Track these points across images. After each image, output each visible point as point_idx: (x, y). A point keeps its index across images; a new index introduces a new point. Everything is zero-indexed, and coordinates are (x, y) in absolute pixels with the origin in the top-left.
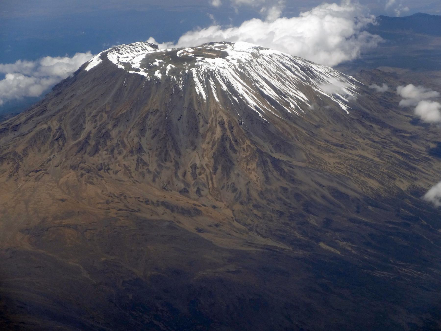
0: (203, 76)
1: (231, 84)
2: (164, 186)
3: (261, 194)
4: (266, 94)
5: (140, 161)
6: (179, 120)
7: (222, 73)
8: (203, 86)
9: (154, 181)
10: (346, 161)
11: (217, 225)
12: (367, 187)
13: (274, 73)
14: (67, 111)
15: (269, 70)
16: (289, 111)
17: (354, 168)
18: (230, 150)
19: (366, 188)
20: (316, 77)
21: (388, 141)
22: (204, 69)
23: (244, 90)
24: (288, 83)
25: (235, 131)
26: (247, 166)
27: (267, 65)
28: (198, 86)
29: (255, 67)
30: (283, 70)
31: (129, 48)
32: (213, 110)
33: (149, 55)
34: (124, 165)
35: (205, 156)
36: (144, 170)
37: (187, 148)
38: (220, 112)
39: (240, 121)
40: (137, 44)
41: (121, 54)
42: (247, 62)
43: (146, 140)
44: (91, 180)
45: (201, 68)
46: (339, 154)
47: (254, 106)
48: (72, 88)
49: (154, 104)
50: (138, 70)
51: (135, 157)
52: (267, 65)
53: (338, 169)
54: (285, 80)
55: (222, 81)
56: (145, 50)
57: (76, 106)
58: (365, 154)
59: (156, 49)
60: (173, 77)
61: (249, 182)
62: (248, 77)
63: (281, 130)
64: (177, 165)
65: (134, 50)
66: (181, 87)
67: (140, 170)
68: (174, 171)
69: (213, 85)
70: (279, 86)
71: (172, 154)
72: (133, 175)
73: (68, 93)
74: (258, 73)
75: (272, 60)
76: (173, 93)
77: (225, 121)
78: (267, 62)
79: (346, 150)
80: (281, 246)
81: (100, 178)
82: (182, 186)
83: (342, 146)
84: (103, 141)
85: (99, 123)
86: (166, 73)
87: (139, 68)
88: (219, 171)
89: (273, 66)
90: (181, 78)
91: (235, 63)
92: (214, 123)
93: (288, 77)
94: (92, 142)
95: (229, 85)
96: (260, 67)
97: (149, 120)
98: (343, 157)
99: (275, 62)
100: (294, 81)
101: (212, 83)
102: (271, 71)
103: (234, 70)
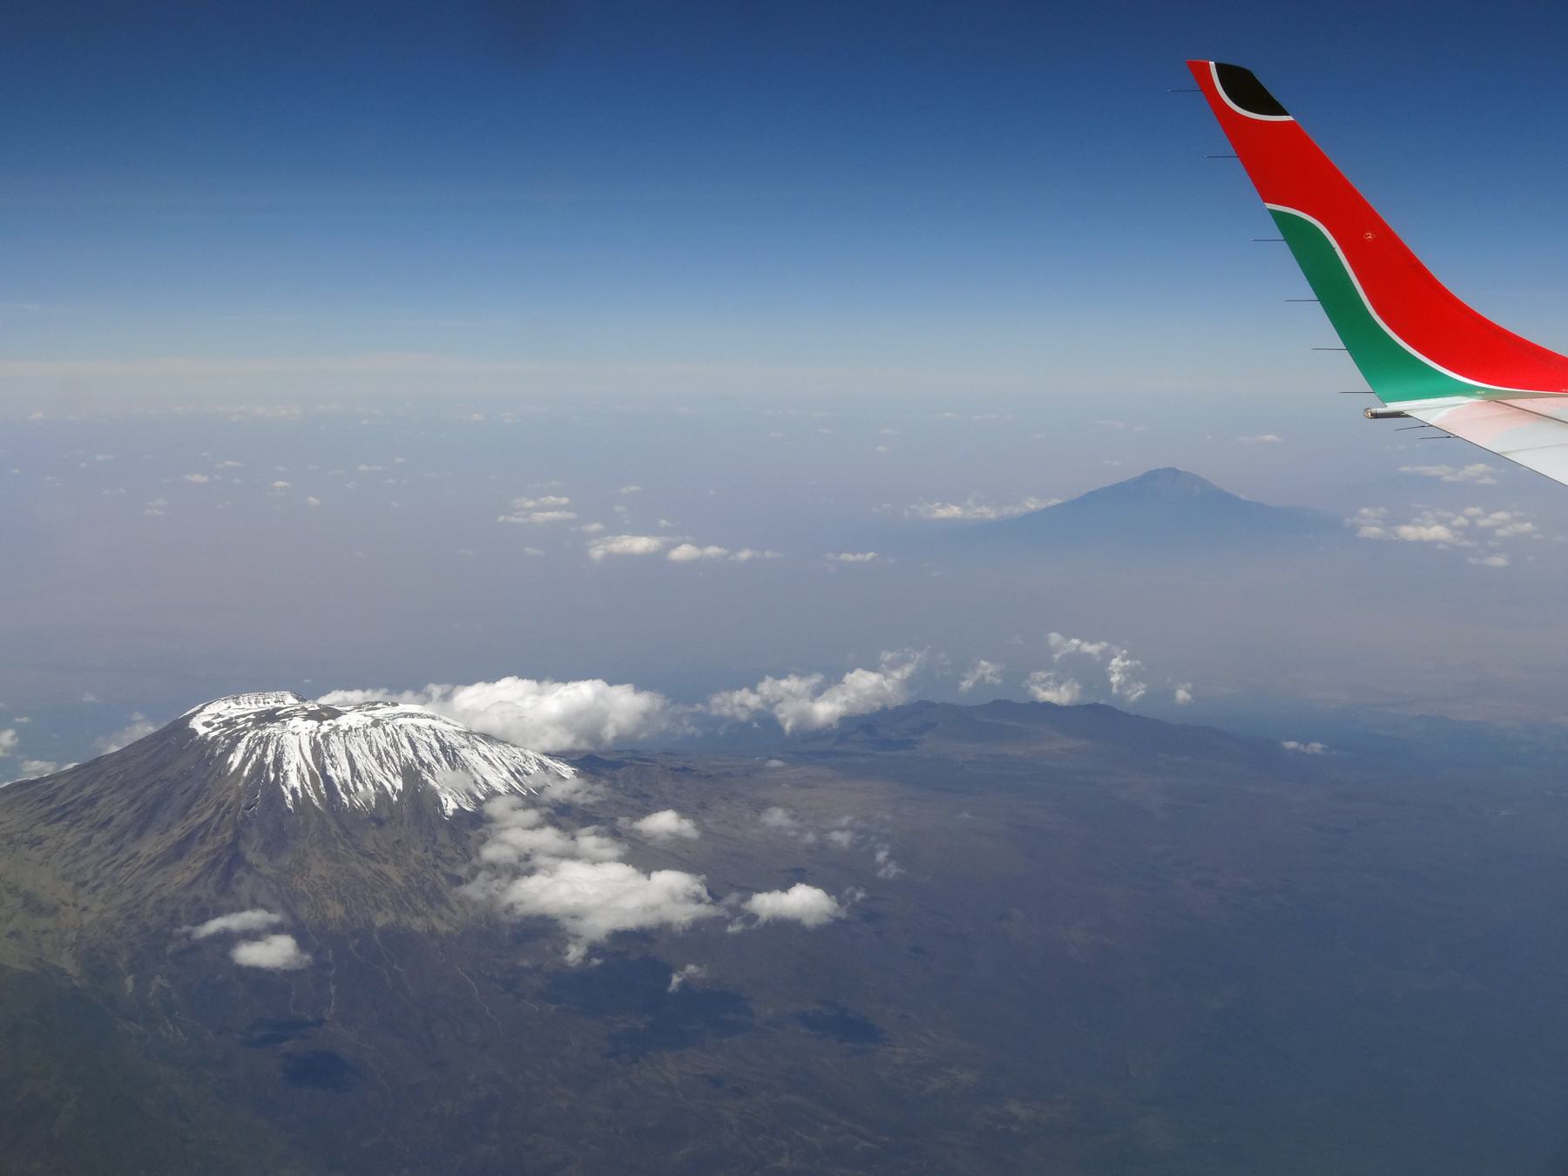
24: (390, 764)
102: (377, 747)
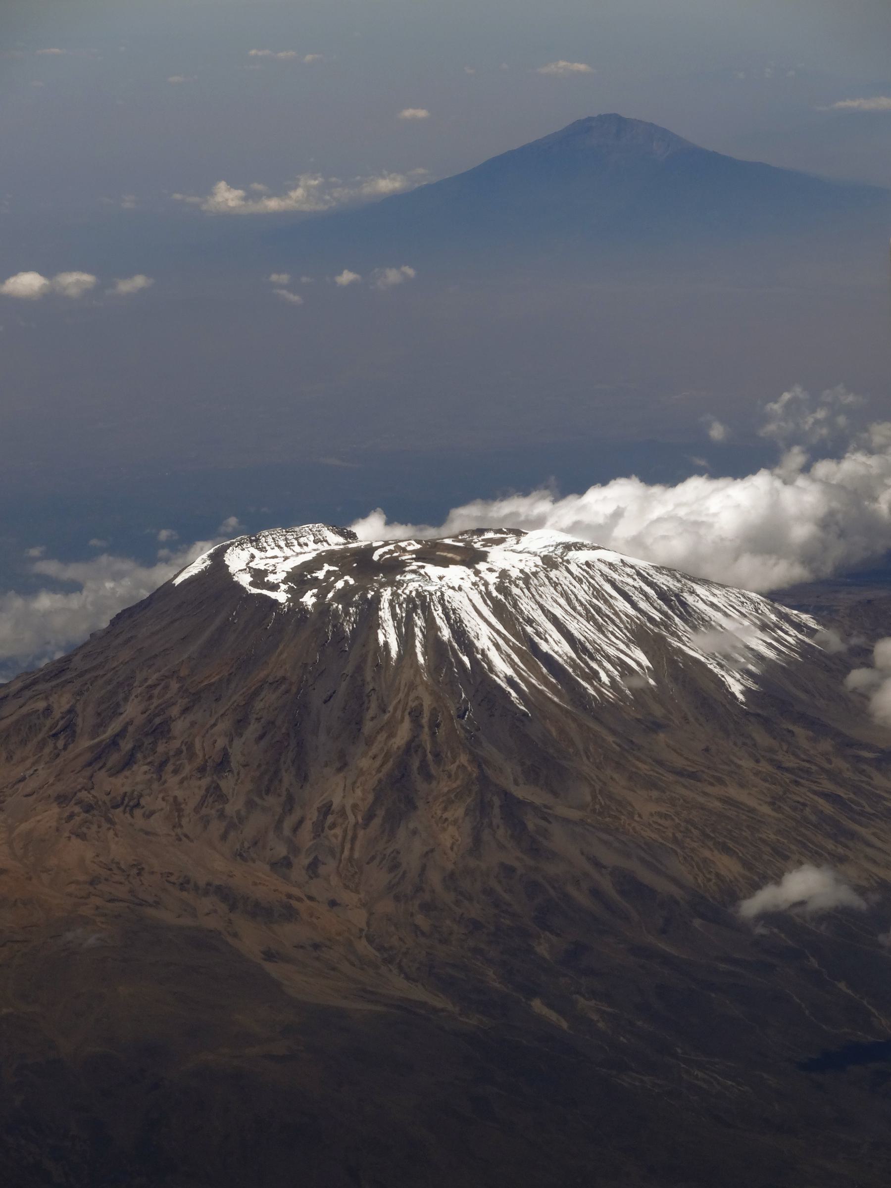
0: (404, 606)
1: (464, 625)
2: (241, 850)
3: (450, 879)
4: (545, 651)
5: (216, 793)
6: (325, 702)
7: (448, 601)
8: (398, 628)
9: (224, 837)
10: (684, 810)
11: (316, 946)
12: (710, 872)
13: (581, 604)
14: (101, 672)
15: (572, 597)
16: (591, 691)
17: (696, 828)
18: (419, 774)
19: (705, 877)
20: (690, 615)
21: (814, 768)
22: (411, 590)
23: (494, 640)
24: (611, 627)
25: (441, 733)
26: (443, 814)
27: (570, 586)
28: (385, 628)
29: (536, 590)
30: (609, 598)
31: (284, 537)
32: (406, 683)
33: (323, 554)
34: (175, 798)
35: (358, 787)
36: (213, 812)
37: (326, 765)
38: (420, 688)
39: (460, 710)
40: (306, 527)
41: (263, 549)
42: (523, 576)
43: (244, 744)
44: (84, 829)
45: (404, 587)
46: (674, 795)
47: (506, 676)
48: (134, 621)
49: (280, 666)
50: (274, 587)
51: (205, 782)
52: (570, 586)
53: (656, 829)
54: (607, 620)
55: (445, 619)
56: (321, 541)
57: (122, 663)
58: (742, 796)
59: (350, 541)
60: (337, 607)
61: (432, 851)
62: (512, 612)
63: (554, 734)
64: (290, 803)
65: (295, 543)
66: (349, 629)
67: (204, 811)
68: (277, 817)
69: (420, 628)
70: (587, 632)
71: (288, 778)
72: (184, 821)
73: (121, 633)
74: (541, 602)
75: (587, 573)
76: (327, 642)
77: (425, 709)
78: (574, 578)
79: (699, 784)
80: (439, 1002)
81: (106, 826)
82: (282, 850)
83: (692, 776)
84: (150, 742)
85: (155, 702)
86: (327, 596)
87: (279, 582)
88: (377, 822)
89: (586, 588)
90: (351, 610)
91: (492, 578)
92: (399, 714)
93: (616, 614)
94: (126, 745)
95: (459, 628)
96: (552, 589)
97: (262, 700)
98: (682, 801)
99: (596, 579)
100: (628, 623)
101: (420, 622)
102: (577, 600)
103: (483, 594)
